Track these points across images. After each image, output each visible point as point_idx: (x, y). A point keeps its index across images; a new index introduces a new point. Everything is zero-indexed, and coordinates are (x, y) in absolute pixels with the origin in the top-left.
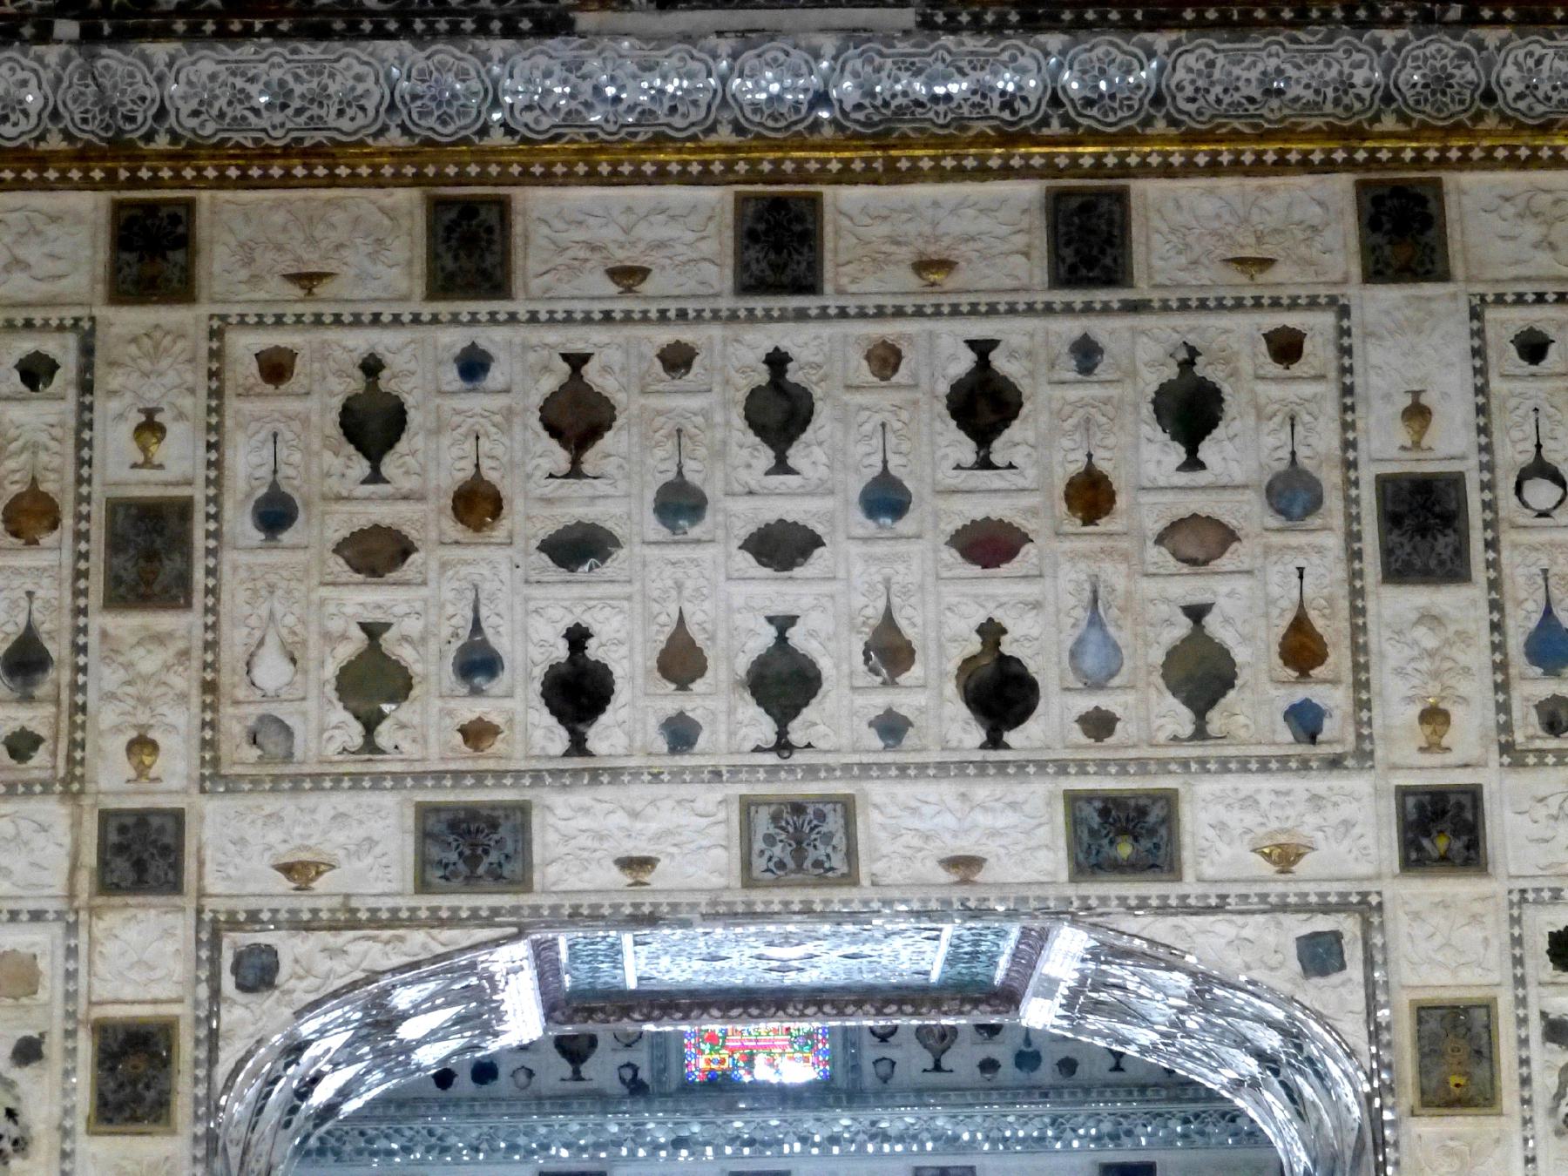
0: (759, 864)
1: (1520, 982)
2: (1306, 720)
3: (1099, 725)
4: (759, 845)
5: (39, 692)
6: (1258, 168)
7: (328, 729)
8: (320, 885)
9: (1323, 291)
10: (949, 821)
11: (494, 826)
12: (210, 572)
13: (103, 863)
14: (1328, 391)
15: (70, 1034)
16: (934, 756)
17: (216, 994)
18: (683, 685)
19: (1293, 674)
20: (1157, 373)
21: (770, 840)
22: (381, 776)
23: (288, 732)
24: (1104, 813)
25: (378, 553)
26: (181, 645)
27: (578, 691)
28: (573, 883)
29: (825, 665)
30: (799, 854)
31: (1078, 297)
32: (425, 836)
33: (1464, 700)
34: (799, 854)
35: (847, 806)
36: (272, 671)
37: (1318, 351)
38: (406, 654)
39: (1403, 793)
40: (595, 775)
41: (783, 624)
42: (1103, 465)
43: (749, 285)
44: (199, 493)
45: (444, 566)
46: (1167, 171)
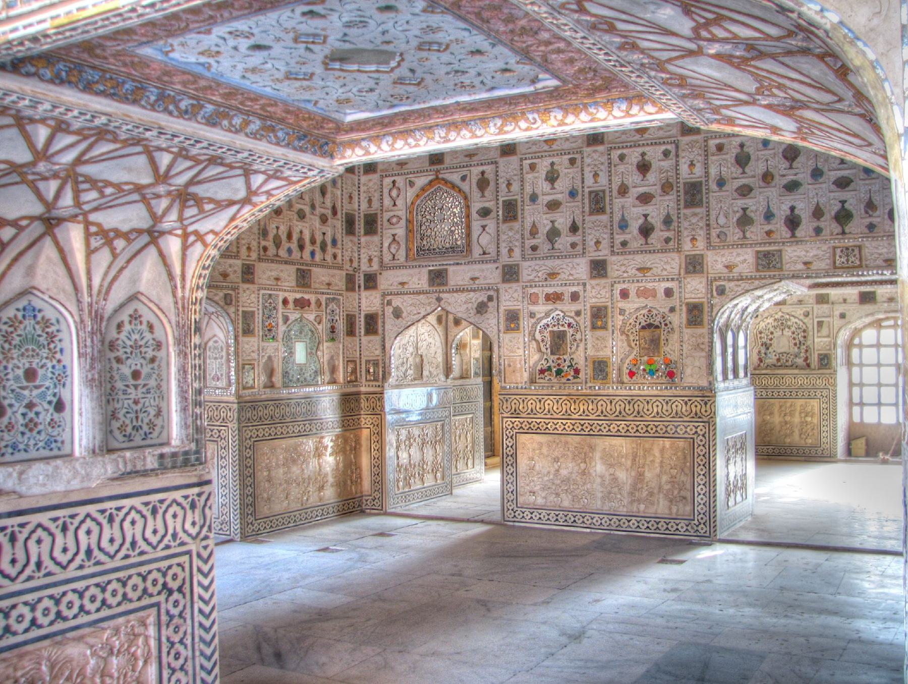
0: (838, 262)
4: (837, 258)
5: (672, 228)
7: (734, 234)
8: (734, 270)
10: (885, 250)
11: (774, 255)
12: (707, 198)
13: (686, 267)
15: (681, 306)
17: (712, 296)
18: (818, 219)
21: (840, 257)
22: (746, 244)
23: (726, 235)
25: (745, 191)
26: (700, 216)
27: (793, 222)
28: (793, 268)
29: (854, 212)
30: (848, 261)
32: (758, 258)
34: (848, 261)
35: (860, 247)
36: (722, 220)
38: (752, 215)
40: (797, 242)
41: (843, 202)
44: (703, 180)
45: (760, 193)
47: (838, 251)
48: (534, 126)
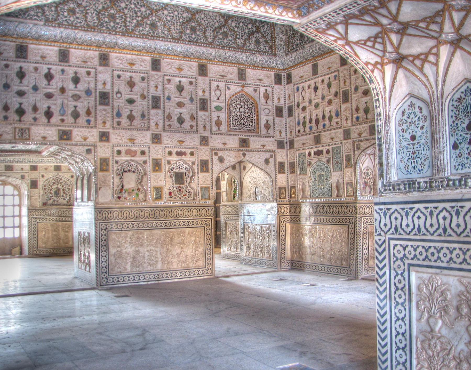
1: (113, 156)
2: (88, 122)
3: (63, 121)
4: (17, 133)
6: (87, 50)
9: (94, 67)
14: (94, 79)
16: (41, 123)
19: (87, 115)
20: (72, 75)
21: (18, 133)
24: (63, 132)
31: (63, 64)
33: (108, 121)
34: (22, 135)
35: (29, 130)
37: (93, 74)
39: (100, 132)
41: (21, 104)
42: (65, 86)
43: (17, 57)
46: (75, 48)
47: (17, 130)
48: (238, 6)
